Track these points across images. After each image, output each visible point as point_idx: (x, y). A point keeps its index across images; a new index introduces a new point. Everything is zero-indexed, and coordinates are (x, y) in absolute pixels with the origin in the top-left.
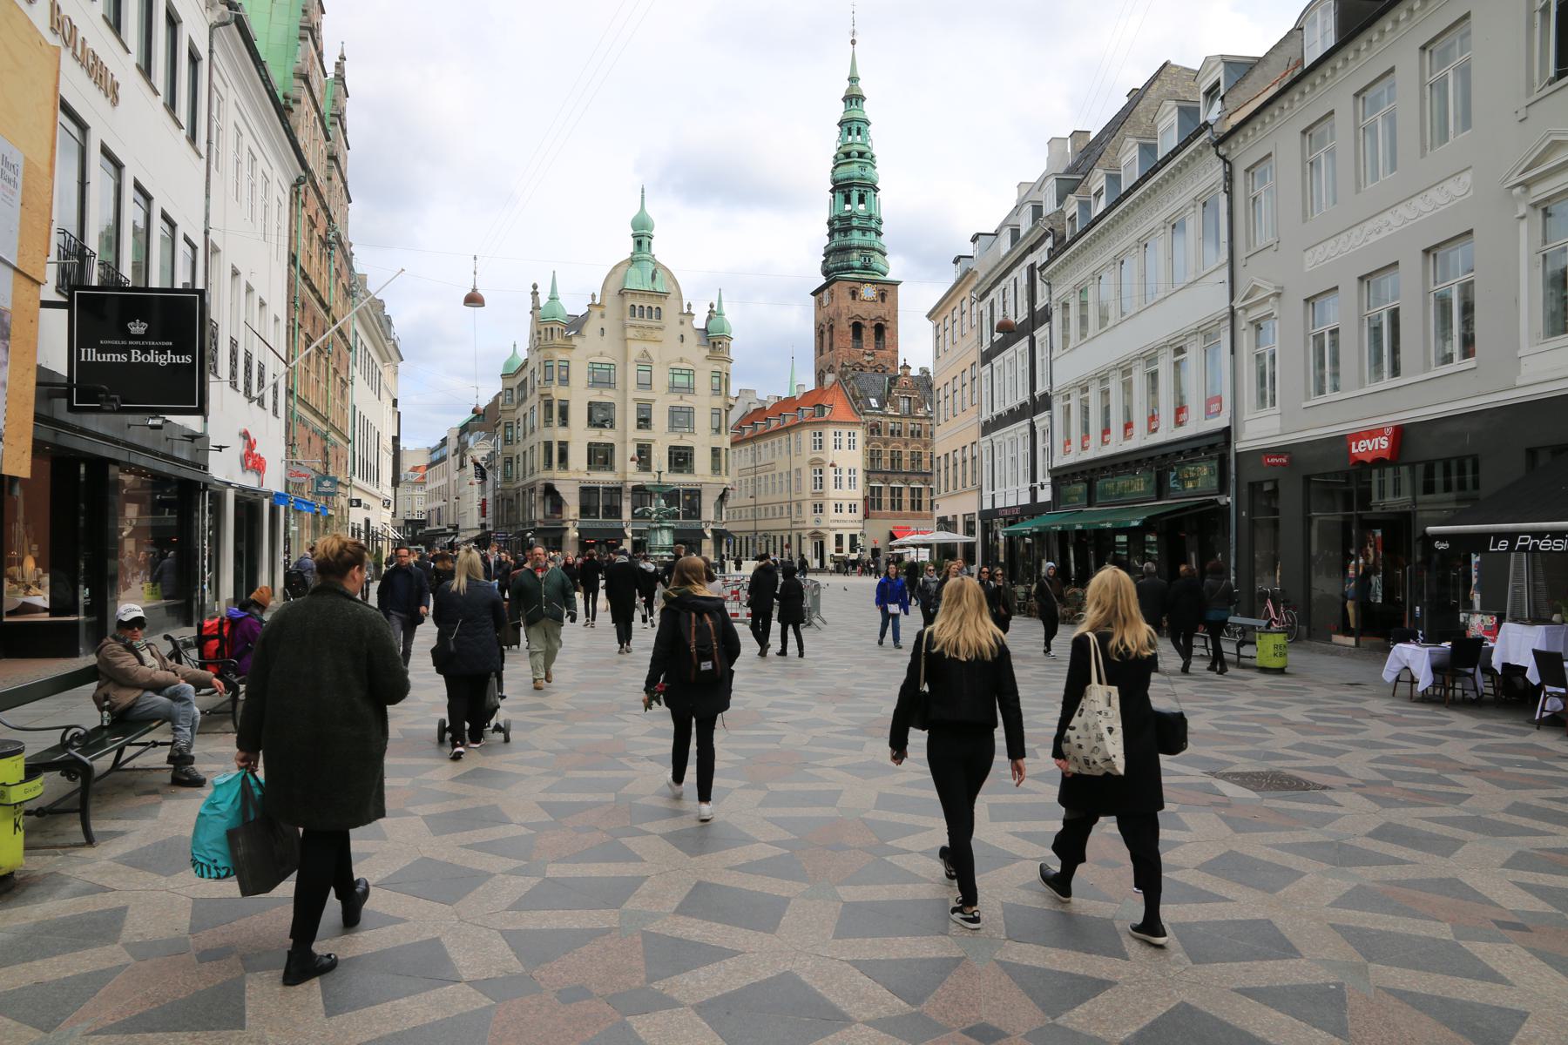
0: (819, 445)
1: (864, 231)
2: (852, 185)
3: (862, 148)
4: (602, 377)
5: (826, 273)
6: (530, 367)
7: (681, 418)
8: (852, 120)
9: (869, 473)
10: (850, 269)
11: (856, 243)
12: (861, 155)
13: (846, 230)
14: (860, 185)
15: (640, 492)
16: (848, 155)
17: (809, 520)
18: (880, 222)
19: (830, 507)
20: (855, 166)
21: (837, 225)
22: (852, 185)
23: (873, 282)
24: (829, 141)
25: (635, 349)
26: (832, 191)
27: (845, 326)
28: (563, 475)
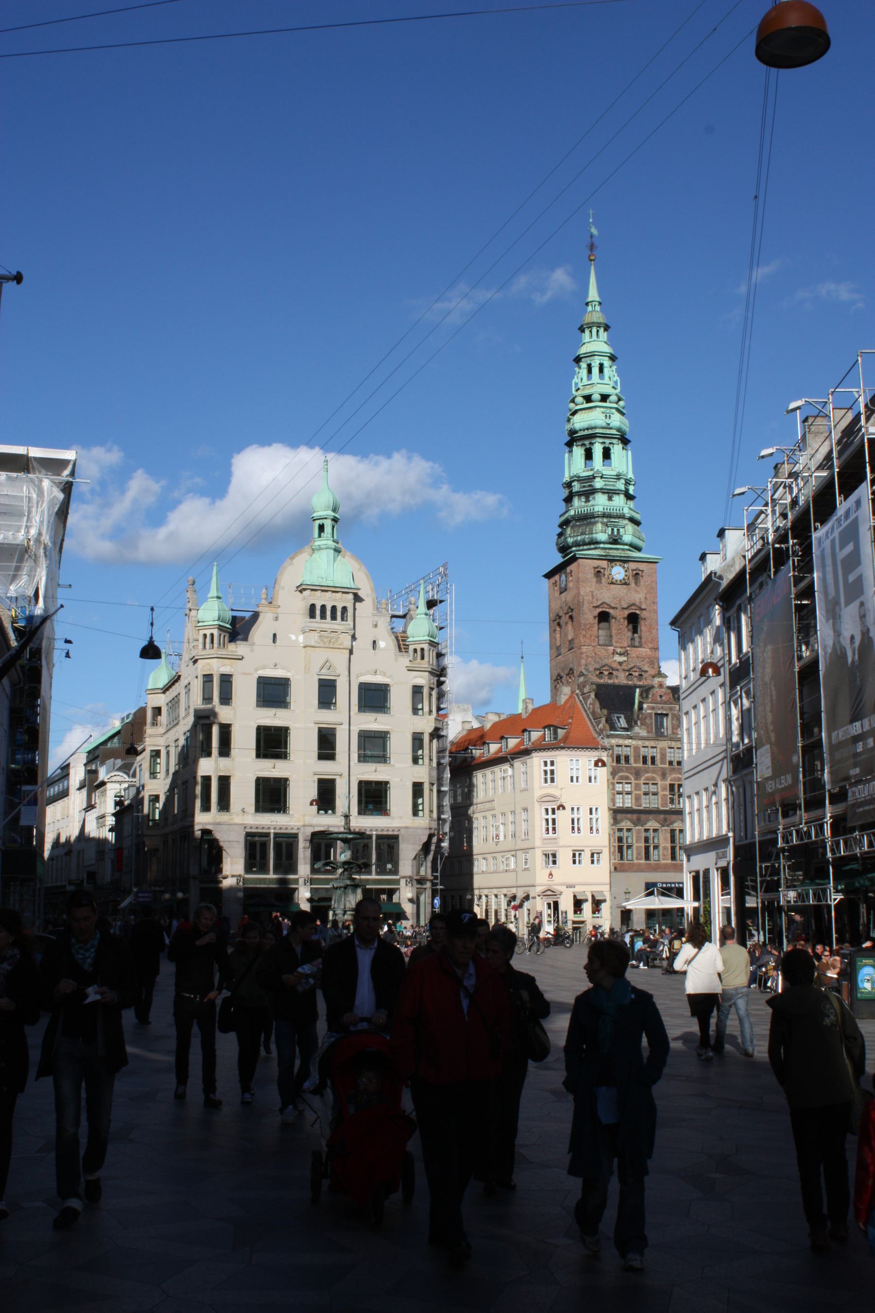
0: (550, 777)
1: (610, 493)
2: (593, 436)
3: (607, 390)
4: (273, 692)
5: (564, 549)
6: (183, 682)
7: (373, 745)
8: (592, 355)
9: (617, 813)
10: (594, 542)
11: (599, 509)
12: (604, 398)
13: (589, 493)
14: (604, 436)
15: (321, 843)
16: (588, 398)
17: (541, 877)
19: (564, 857)
21: (576, 487)
22: (593, 436)
23: (624, 561)
27: (589, 616)
28: (224, 817)
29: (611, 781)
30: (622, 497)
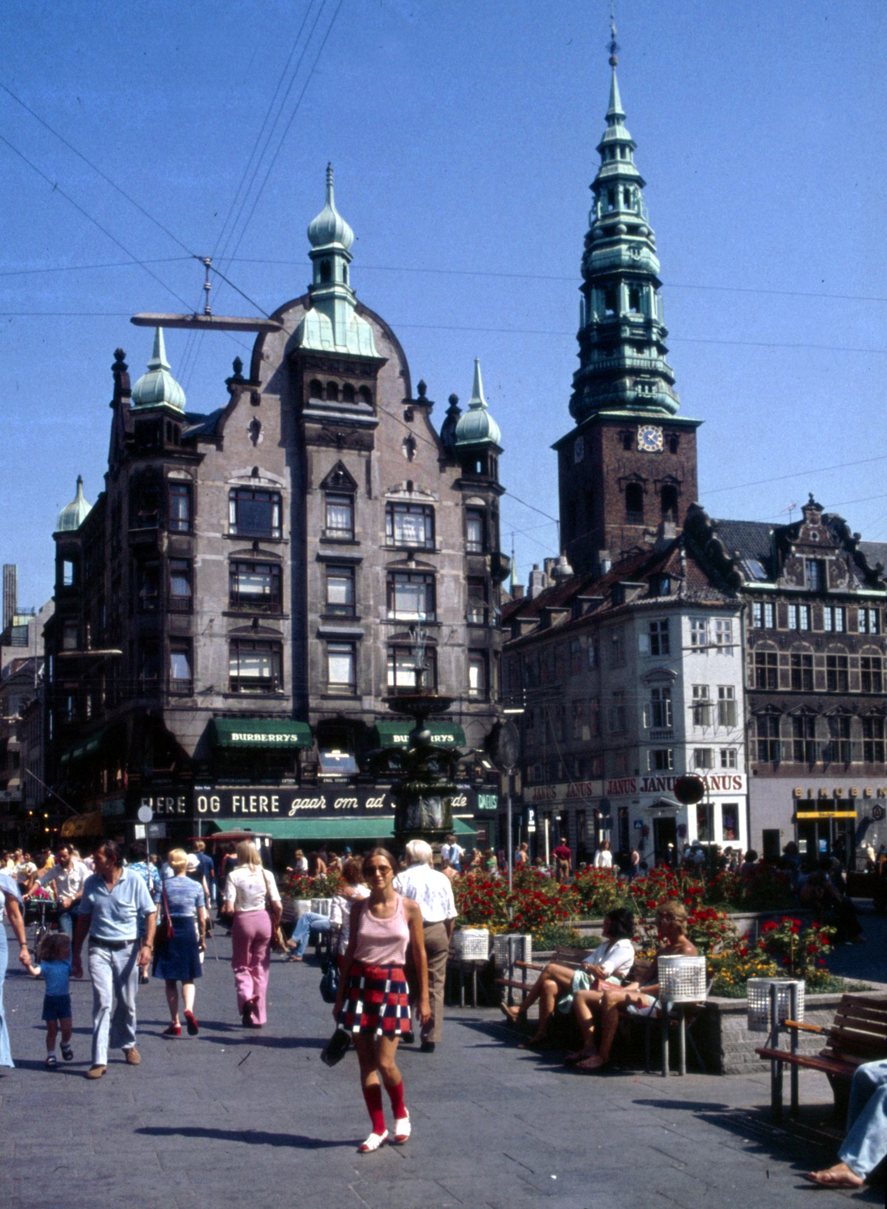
1: (641, 345)
11: (628, 362)
18: (663, 333)
20: (624, 247)
24: (579, 213)
25: (323, 461)
26: (585, 289)
29: (748, 650)
30: (654, 351)
